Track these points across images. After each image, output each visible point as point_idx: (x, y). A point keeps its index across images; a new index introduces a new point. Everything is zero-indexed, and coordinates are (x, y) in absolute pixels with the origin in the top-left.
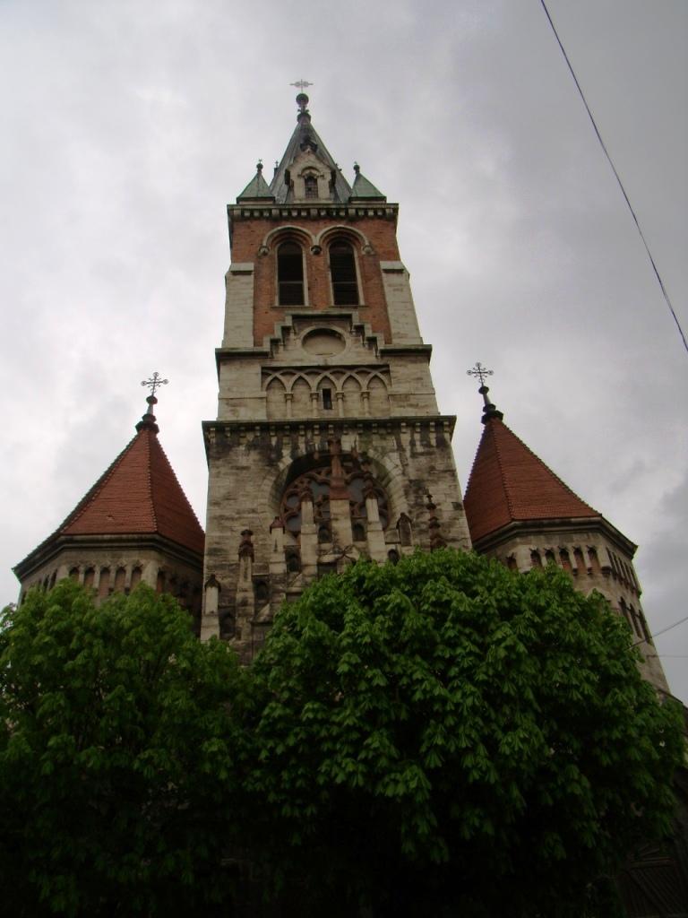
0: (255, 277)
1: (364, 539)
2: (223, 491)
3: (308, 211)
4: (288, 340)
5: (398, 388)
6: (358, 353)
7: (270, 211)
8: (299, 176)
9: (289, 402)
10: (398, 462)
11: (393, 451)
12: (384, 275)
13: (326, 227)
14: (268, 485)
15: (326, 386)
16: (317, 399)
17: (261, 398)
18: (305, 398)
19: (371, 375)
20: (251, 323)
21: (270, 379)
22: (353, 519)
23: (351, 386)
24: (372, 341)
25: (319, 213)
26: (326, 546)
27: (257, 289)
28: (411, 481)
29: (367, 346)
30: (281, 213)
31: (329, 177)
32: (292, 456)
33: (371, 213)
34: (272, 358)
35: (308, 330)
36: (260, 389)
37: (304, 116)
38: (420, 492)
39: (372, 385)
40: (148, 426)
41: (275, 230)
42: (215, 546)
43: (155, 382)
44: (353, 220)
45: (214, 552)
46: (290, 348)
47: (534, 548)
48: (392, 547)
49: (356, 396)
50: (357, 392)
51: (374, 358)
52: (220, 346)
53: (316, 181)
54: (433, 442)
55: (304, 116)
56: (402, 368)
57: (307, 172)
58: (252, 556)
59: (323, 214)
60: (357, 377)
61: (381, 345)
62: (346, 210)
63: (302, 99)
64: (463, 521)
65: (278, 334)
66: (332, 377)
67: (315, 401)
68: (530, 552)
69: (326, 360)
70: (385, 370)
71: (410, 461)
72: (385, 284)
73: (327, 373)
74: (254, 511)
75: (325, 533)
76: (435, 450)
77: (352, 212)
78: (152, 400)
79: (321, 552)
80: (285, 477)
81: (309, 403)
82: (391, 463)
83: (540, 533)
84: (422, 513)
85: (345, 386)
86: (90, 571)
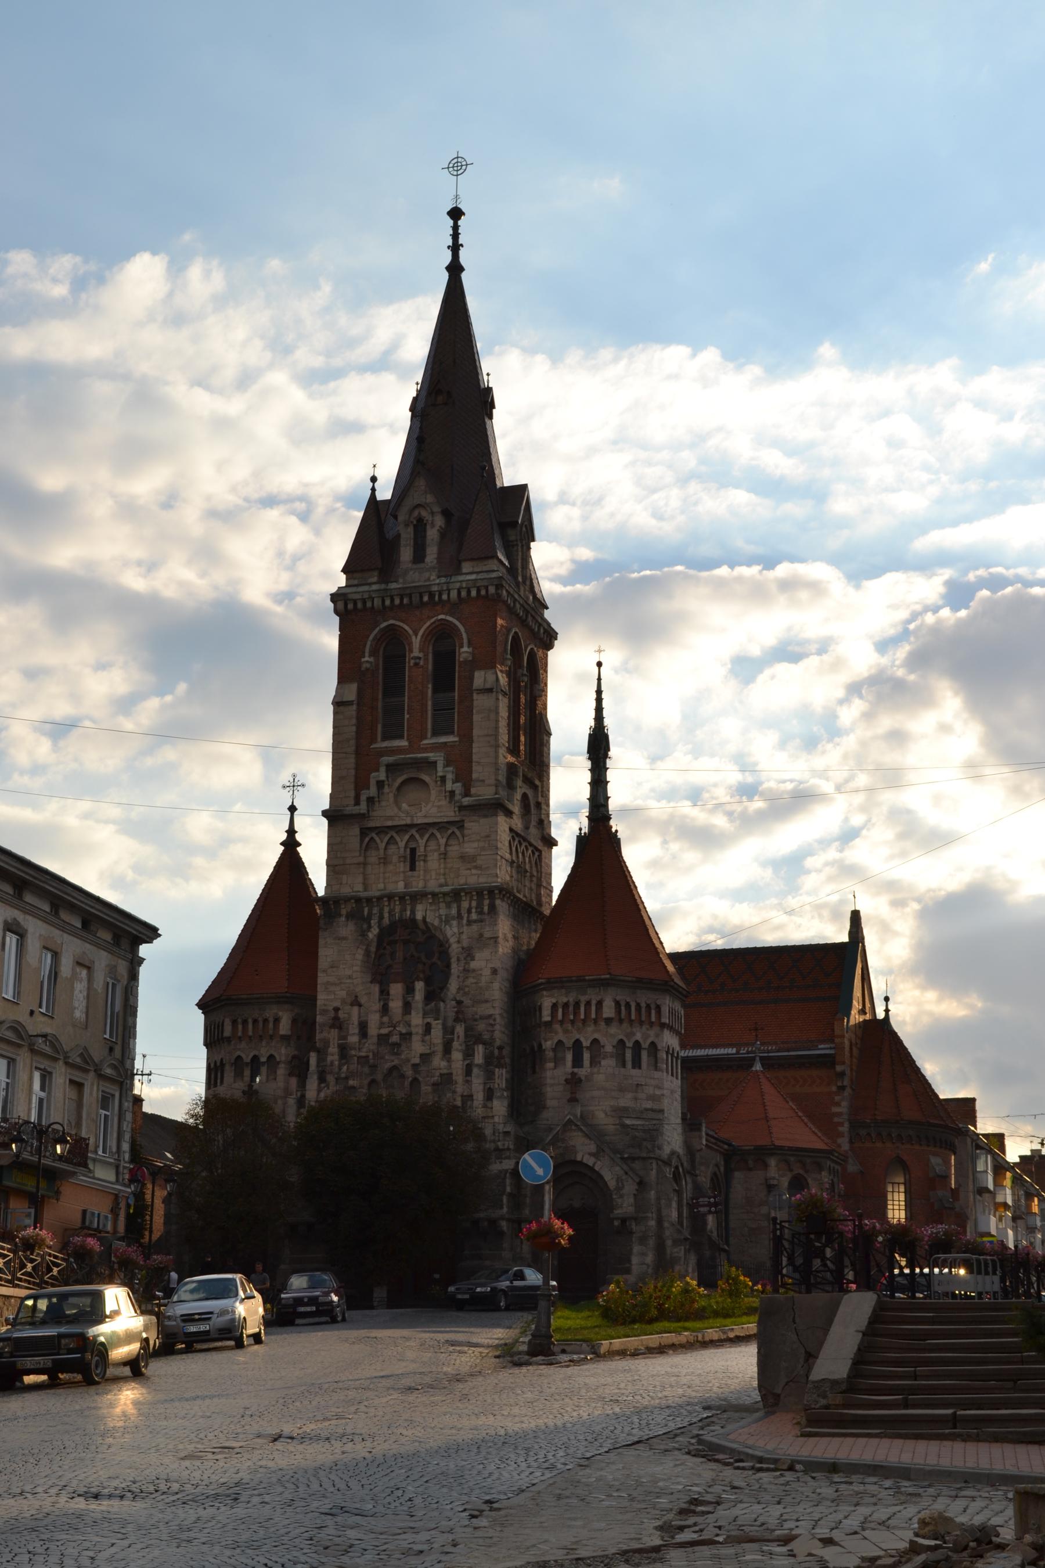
0: (358, 704)
1: (410, 1014)
2: (329, 960)
3: (410, 596)
4: (383, 793)
5: (470, 848)
6: (439, 807)
7: (373, 599)
8: (407, 525)
9: (382, 865)
10: (455, 930)
11: (453, 918)
12: (475, 696)
13: (430, 618)
14: (360, 954)
15: (412, 845)
16: (405, 862)
17: (359, 864)
18: (395, 859)
19: (450, 832)
20: (353, 772)
21: (367, 839)
22: (404, 997)
23: (432, 845)
24: (452, 793)
25: (421, 597)
26: (385, 1019)
27: (359, 719)
28: (463, 948)
29: (448, 799)
30: (383, 601)
31: (439, 521)
32: (379, 926)
33: (474, 593)
34: (369, 817)
35: (400, 780)
36: (357, 854)
37: (455, 269)
38: (469, 959)
39: (451, 842)
40: (291, 844)
41: (378, 629)
42: (325, 1008)
43: (294, 786)
44: (454, 608)
45: (324, 1012)
46: (383, 804)
47: (554, 1001)
48: (429, 1020)
49: (436, 854)
50: (435, 850)
51: (452, 814)
52: (327, 807)
53: (426, 524)
54: (486, 909)
55: (455, 269)
56: (472, 824)
57: (416, 513)
58: (340, 1028)
59: (426, 598)
60: (438, 835)
61: (457, 797)
62: (449, 590)
63: (456, 214)
64: (496, 985)
65: (373, 791)
66: (417, 836)
67: (402, 864)
68: (551, 1004)
69: (412, 820)
70: (460, 825)
71: (465, 928)
72: (474, 711)
73: (413, 831)
74: (350, 977)
75: (385, 1010)
76: (486, 917)
77: (454, 594)
78: (292, 809)
79: (382, 1025)
80: (375, 944)
81: (398, 864)
82: (451, 931)
83: (562, 987)
84: (467, 978)
85: (429, 844)
86: (245, 1022)
